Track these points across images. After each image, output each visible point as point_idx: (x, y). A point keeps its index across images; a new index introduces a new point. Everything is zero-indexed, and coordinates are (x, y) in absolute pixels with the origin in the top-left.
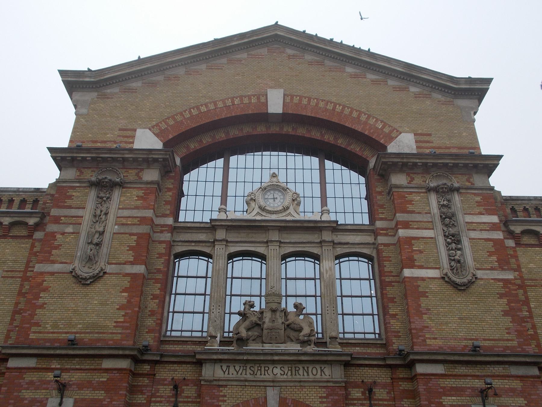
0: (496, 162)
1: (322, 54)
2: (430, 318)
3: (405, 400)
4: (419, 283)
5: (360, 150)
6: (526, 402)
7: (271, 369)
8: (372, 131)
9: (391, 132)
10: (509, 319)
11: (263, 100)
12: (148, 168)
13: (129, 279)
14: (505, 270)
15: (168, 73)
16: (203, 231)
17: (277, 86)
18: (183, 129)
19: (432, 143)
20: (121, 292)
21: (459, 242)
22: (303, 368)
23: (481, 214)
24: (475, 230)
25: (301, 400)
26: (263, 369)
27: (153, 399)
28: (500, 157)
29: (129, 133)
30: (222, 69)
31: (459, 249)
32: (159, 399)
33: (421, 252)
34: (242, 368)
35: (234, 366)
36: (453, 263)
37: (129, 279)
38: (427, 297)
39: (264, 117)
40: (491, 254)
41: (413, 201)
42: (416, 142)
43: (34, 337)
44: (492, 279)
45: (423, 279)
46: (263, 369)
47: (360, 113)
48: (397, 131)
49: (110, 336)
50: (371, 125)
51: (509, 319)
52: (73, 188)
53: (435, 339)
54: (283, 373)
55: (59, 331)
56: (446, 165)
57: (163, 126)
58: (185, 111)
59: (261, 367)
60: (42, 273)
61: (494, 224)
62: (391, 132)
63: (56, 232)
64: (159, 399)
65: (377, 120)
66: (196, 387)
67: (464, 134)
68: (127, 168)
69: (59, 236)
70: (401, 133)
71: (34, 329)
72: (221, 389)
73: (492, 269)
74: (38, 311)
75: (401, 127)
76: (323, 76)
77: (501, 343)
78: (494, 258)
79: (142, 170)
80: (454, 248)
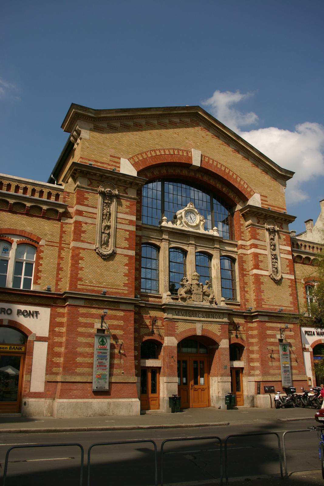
0: (293, 220)
1: (219, 133)
2: (264, 295)
3: (250, 331)
4: (261, 277)
5: (233, 197)
6: (294, 334)
7: (198, 315)
8: (242, 189)
10: (291, 297)
11: (190, 155)
12: (131, 187)
13: (127, 258)
14: (291, 274)
15: (135, 120)
16: (155, 231)
17: (197, 147)
18: (148, 164)
19: (267, 202)
20: (124, 266)
22: (212, 315)
23: (285, 245)
24: (282, 253)
25: (211, 330)
26: (194, 314)
27: (141, 326)
28: (296, 217)
29: (116, 160)
30: (166, 127)
31: (277, 263)
32: (144, 326)
33: (262, 261)
34: (185, 313)
35: (181, 312)
36: (274, 269)
37: (127, 258)
38: (263, 284)
39: (188, 166)
41: (259, 233)
42: (261, 200)
43: (80, 288)
44: (287, 278)
45: (262, 275)
46: (194, 314)
47: (237, 176)
48: (253, 192)
49: (122, 291)
50: (242, 185)
51: (291, 297)
52: (88, 192)
53: (266, 305)
54: (203, 317)
55: (94, 285)
56: (274, 217)
57: (137, 160)
58: (148, 152)
59: (193, 313)
60: (78, 248)
61: (289, 251)
63: (81, 222)
64: (144, 326)
65: (245, 183)
66: (161, 321)
67: (280, 200)
68: (118, 185)
69: (83, 225)
70: (255, 193)
71: (79, 282)
72: (176, 323)
73: (288, 273)
74: (80, 272)
75: (255, 189)
76: (219, 147)
77: (288, 308)
79: (127, 188)
80: (274, 262)
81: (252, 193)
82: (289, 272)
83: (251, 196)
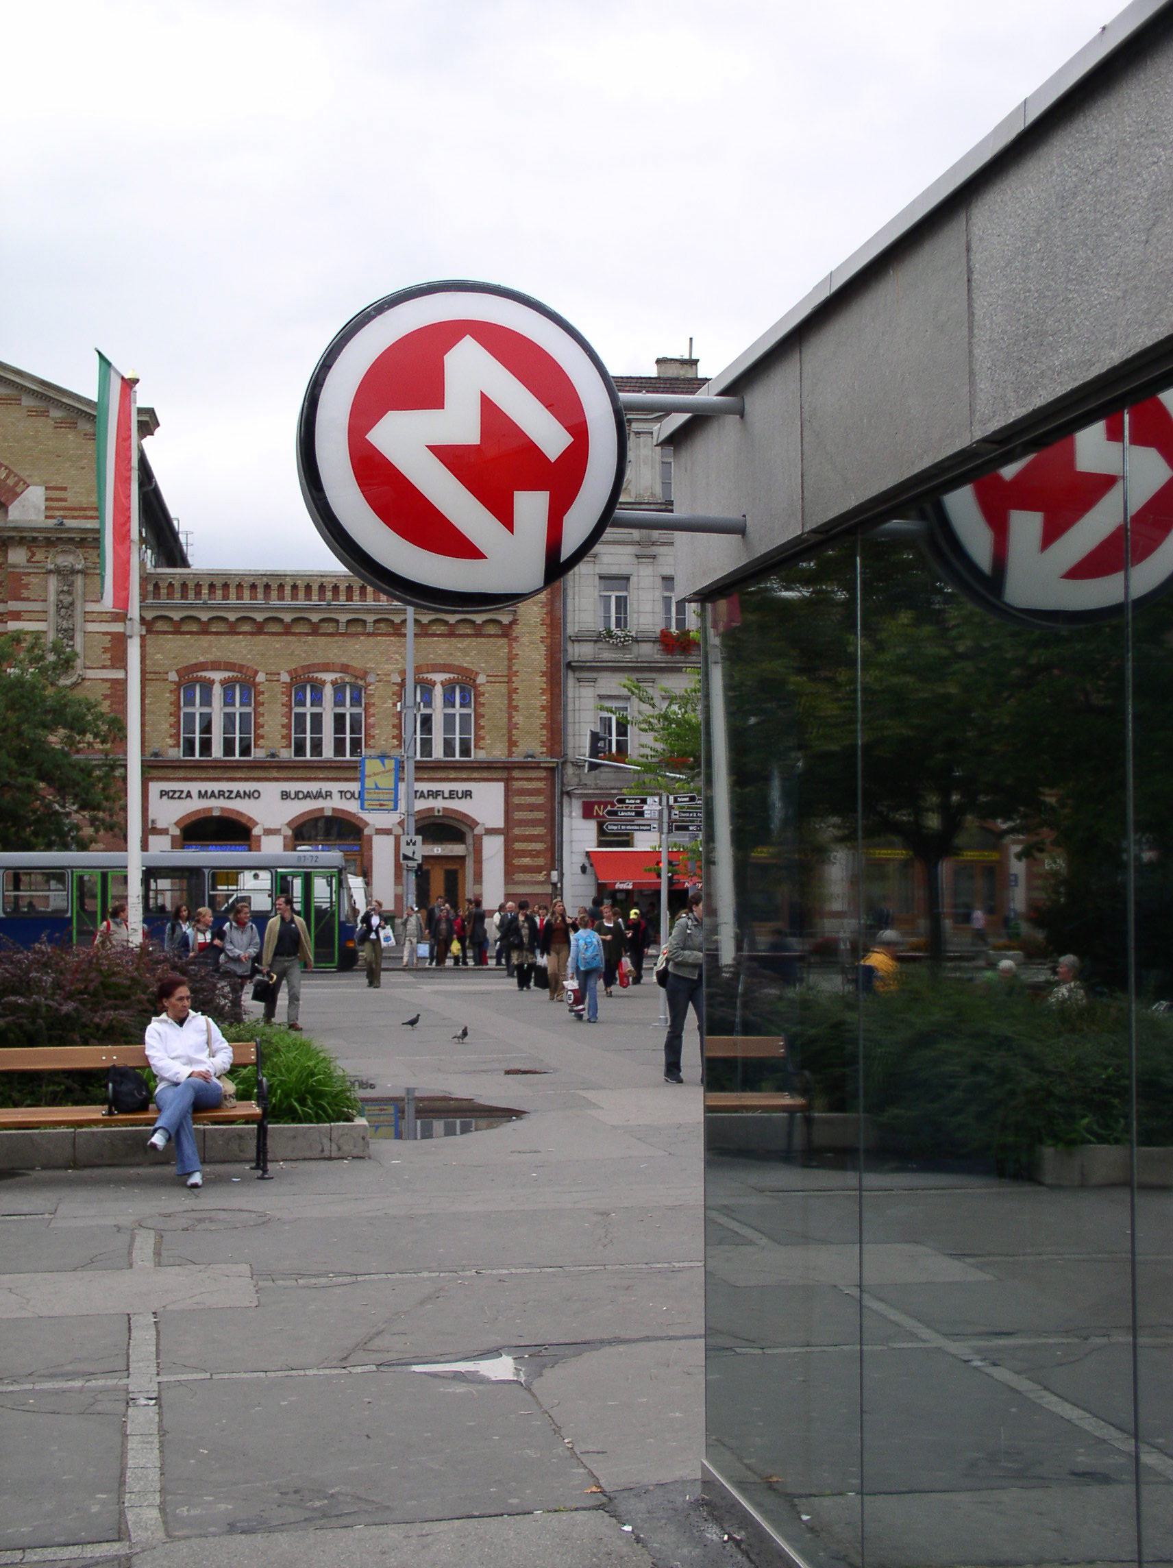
9: (16, 484)
21: (72, 638)
40: (106, 650)
42: (47, 500)
56: (71, 539)
62: (16, 484)
73: (104, 667)
75: (29, 476)
78: (109, 656)
81: (18, 490)
82: (108, 663)
83: (17, 495)
